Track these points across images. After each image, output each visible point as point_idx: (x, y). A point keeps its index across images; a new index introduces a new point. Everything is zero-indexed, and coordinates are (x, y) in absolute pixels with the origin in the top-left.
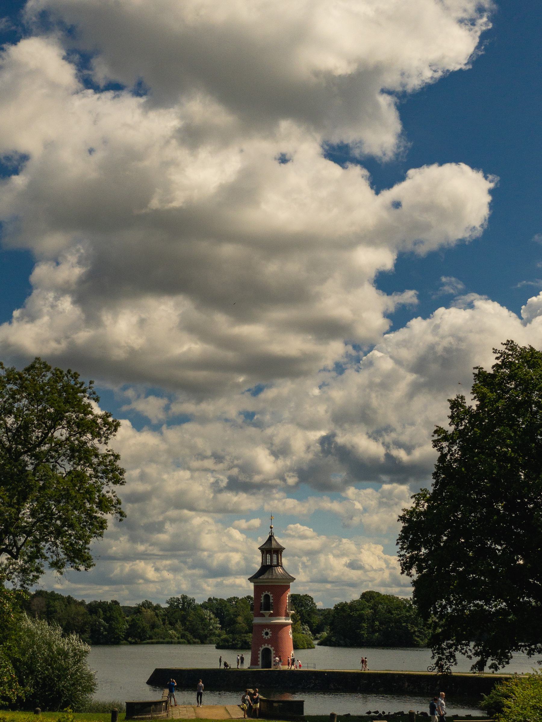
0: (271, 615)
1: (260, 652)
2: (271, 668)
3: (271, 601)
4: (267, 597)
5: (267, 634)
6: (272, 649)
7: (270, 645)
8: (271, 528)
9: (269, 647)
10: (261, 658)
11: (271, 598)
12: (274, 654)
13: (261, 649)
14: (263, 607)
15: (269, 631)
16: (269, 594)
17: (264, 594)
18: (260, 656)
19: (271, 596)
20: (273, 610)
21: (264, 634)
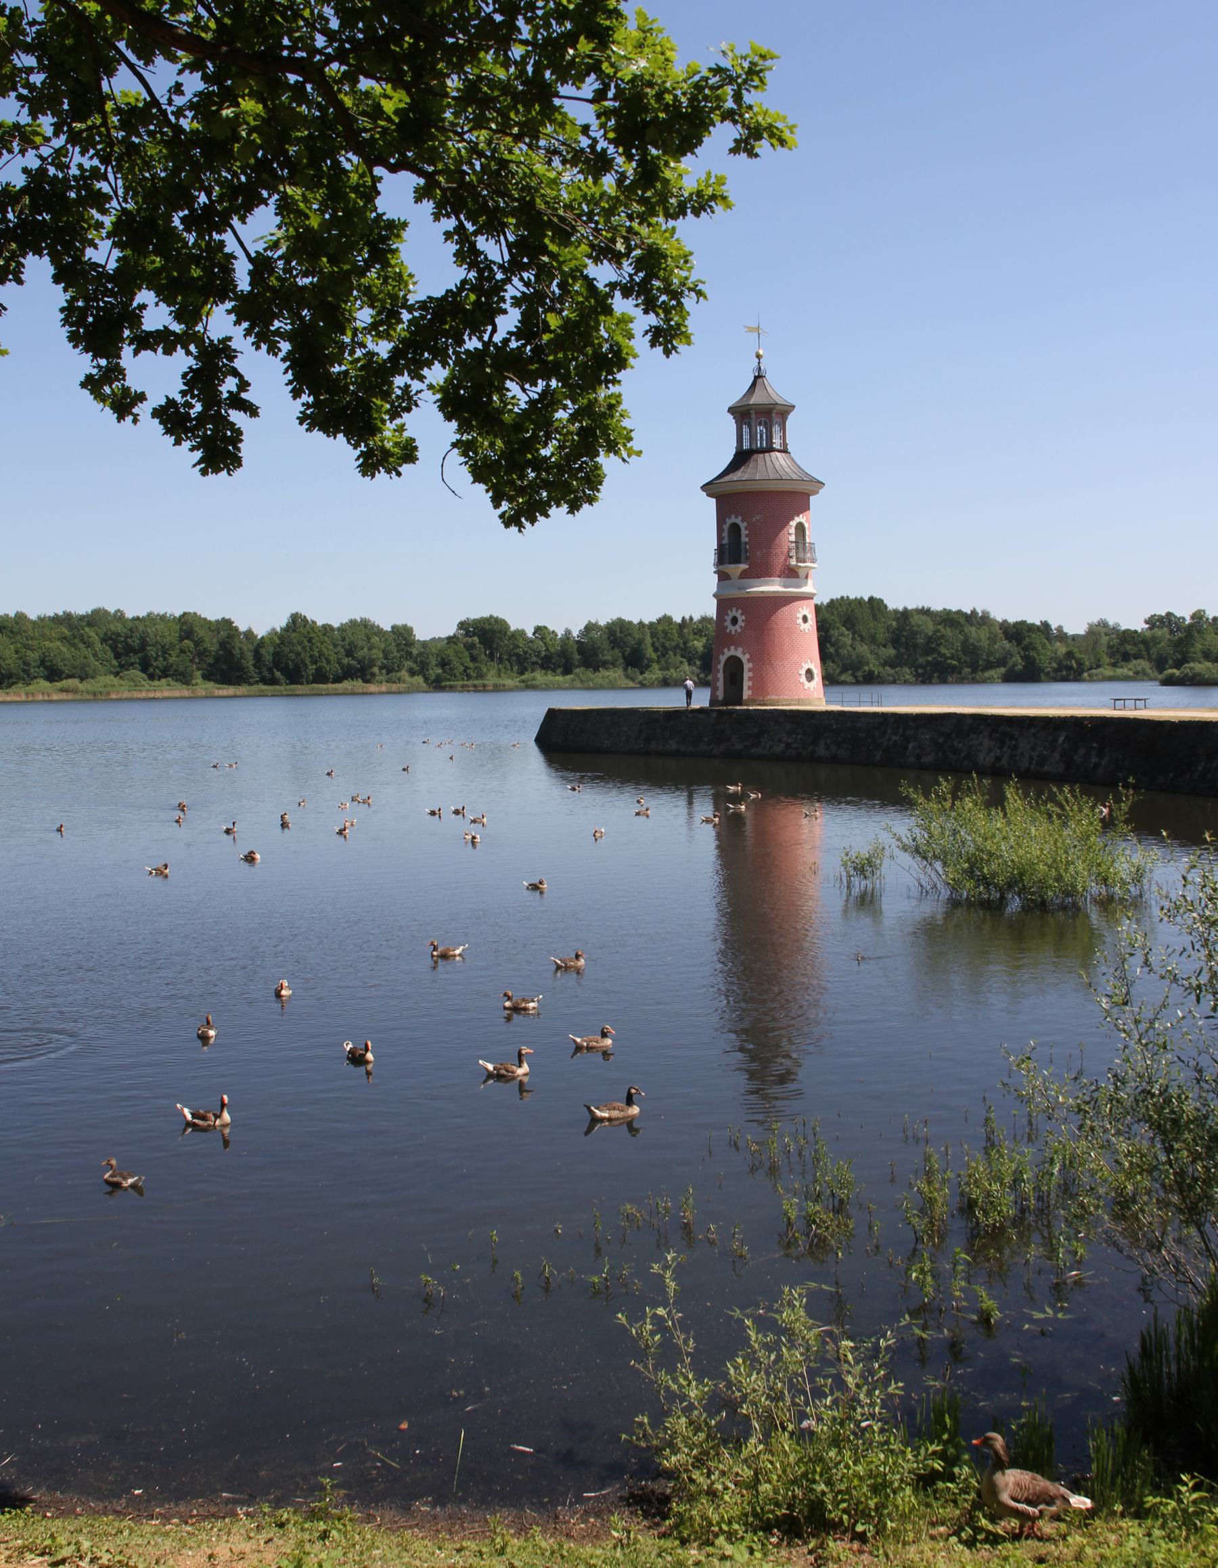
0: (744, 575)
1: (721, 667)
2: (741, 704)
3: (744, 539)
4: (735, 529)
5: (735, 621)
6: (745, 658)
7: (740, 650)
8: (758, 356)
9: (738, 653)
10: (721, 680)
11: (744, 532)
12: (750, 670)
13: (723, 659)
14: (727, 556)
15: (738, 614)
16: (738, 521)
17: (729, 522)
18: (721, 675)
19: (743, 526)
20: (747, 558)
21: (728, 623)
